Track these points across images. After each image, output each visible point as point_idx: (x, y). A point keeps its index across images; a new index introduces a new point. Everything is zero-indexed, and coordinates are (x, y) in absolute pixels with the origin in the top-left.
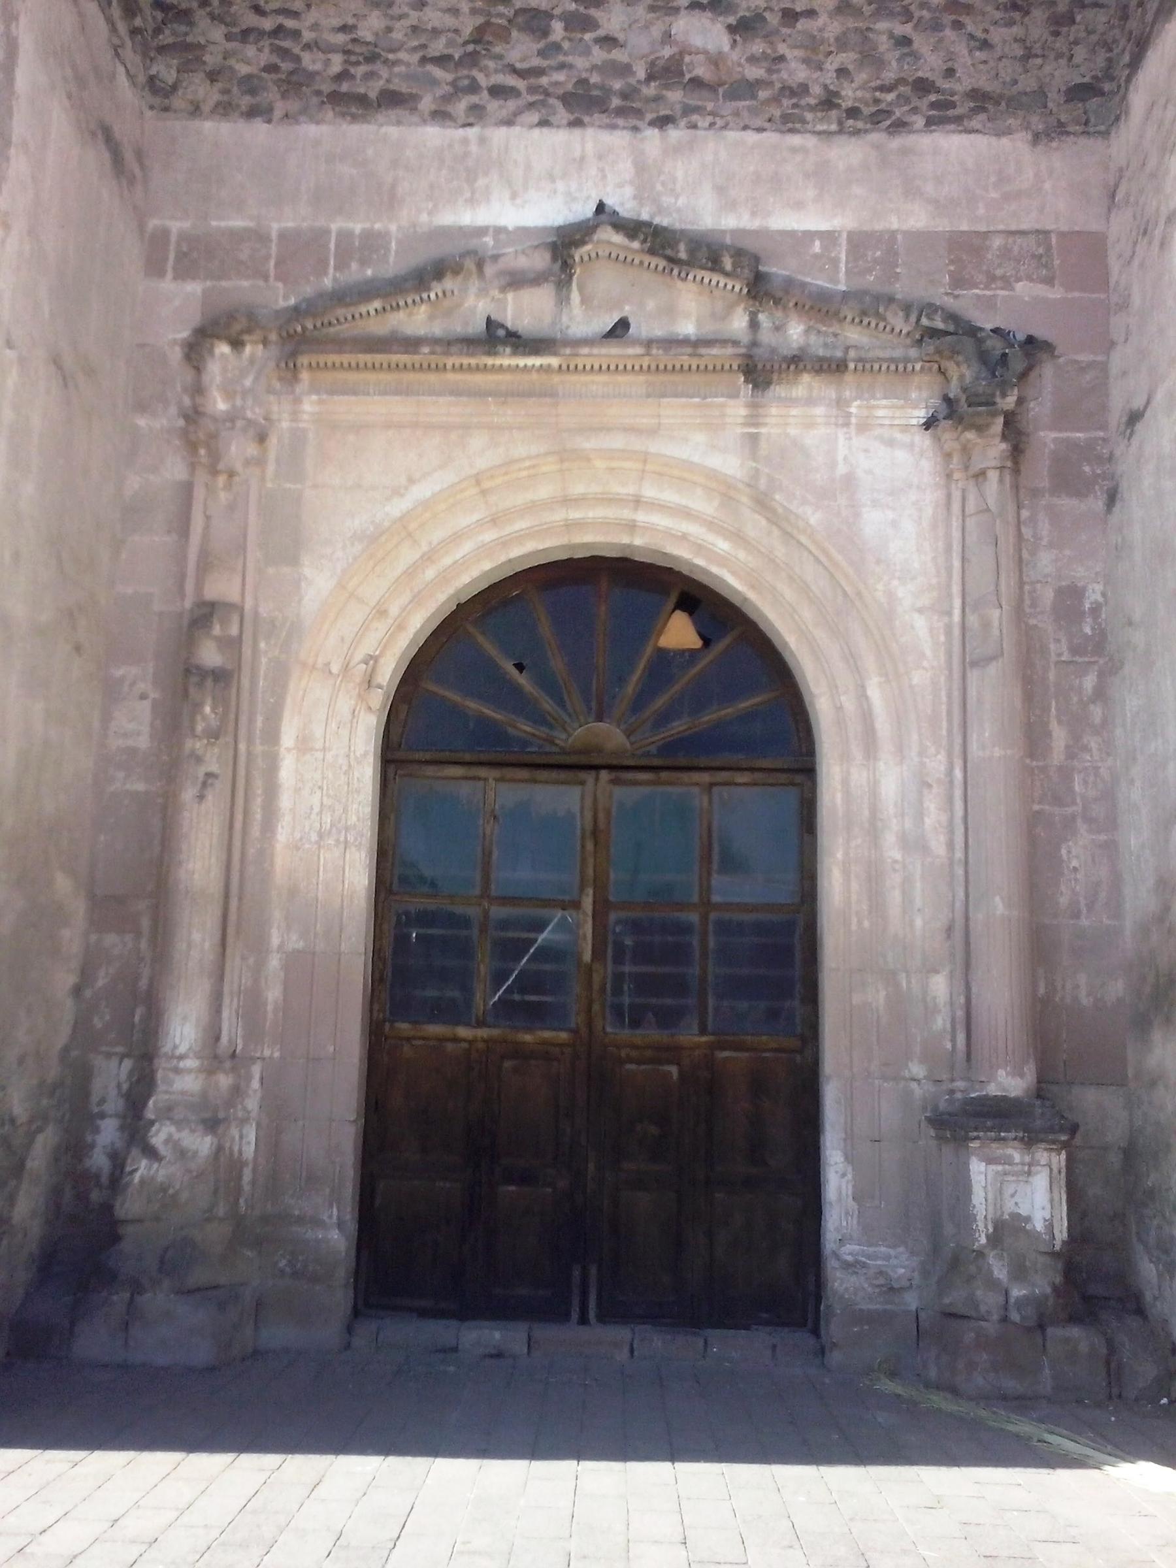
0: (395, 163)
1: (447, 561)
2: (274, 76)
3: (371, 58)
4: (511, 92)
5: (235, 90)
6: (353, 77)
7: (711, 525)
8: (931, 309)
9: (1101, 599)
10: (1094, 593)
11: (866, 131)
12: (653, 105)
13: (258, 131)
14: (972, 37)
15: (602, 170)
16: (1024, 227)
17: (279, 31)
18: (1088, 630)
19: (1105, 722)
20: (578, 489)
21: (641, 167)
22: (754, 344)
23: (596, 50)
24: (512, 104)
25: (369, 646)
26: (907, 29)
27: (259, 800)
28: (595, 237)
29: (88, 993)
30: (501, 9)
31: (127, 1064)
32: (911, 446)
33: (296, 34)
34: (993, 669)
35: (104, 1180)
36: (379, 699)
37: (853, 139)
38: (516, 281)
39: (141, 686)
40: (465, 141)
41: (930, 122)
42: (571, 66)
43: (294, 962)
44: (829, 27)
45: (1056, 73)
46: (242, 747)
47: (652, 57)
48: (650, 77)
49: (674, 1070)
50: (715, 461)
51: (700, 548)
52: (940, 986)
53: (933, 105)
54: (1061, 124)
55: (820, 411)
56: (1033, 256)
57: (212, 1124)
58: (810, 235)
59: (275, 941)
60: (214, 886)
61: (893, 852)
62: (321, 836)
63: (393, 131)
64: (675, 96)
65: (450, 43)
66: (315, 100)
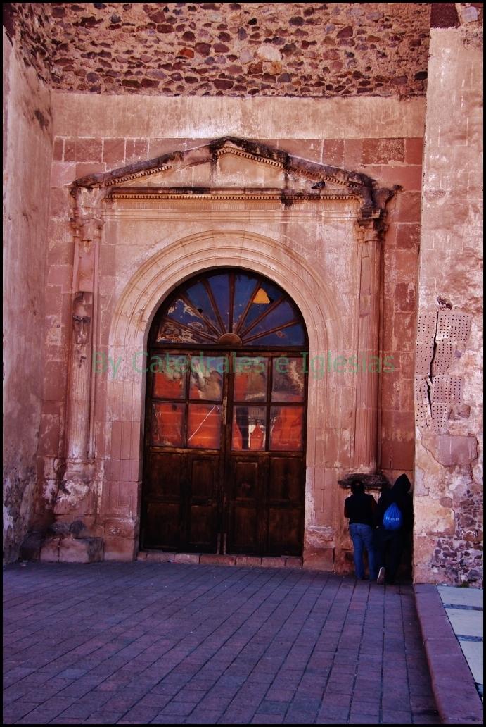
0: (149, 112)
1: (170, 273)
2: (101, 73)
3: (139, 65)
4: (195, 80)
5: (86, 79)
6: (132, 74)
7: (269, 259)
8: (353, 174)
9: (414, 289)
10: (411, 287)
11: (333, 96)
12: (250, 85)
13: (95, 98)
14: (379, 52)
15: (229, 114)
16: (394, 136)
17: (102, 53)
18: (408, 301)
19: (412, 336)
20: (219, 245)
21: (244, 113)
22: (287, 188)
23: (228, 61)
24: (195, 85)
25: (141, 306)
26: (352, 50)
27: (101, 365)
28: (225, 146)
29: (42, 436)
30: (190, 43)
31: (57, 461)
32: (345, 228)
33: (109, 55)
34: (366, 319)
35: (50, 502)
36: (144, 326)
37: (328, 100)
38: (196, 162)
39: (58, 322)
40: (176, 102)
41: (359, 91)
42: (218, 68)
43: (115, 425)
44: (321, 49)
45: (412, 68)
46: (94, 346)
47: (250, 63)
48: (249, 73)
49: (256, 464)
50: (271, 235)
51: (265, 268)
52: (347, 434)
53: (361, 84)
54: (412, 90)
55: (310, 215)
56: (397, 149)
57: (87, 483)
58: (309, 141)
59: (108, 418)
60: (85, 398)
61: (333, 385)
62: (124, 378)
63: (147, 98)
64: (259, 81)
65: (171, 59)
66: (117, 84)
